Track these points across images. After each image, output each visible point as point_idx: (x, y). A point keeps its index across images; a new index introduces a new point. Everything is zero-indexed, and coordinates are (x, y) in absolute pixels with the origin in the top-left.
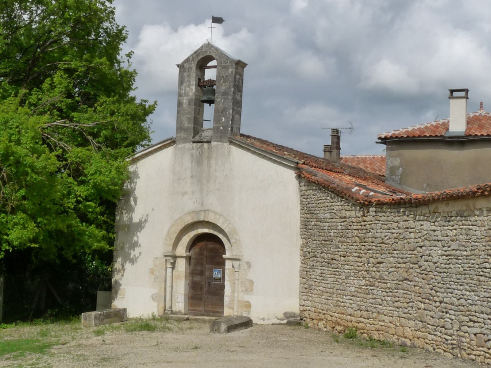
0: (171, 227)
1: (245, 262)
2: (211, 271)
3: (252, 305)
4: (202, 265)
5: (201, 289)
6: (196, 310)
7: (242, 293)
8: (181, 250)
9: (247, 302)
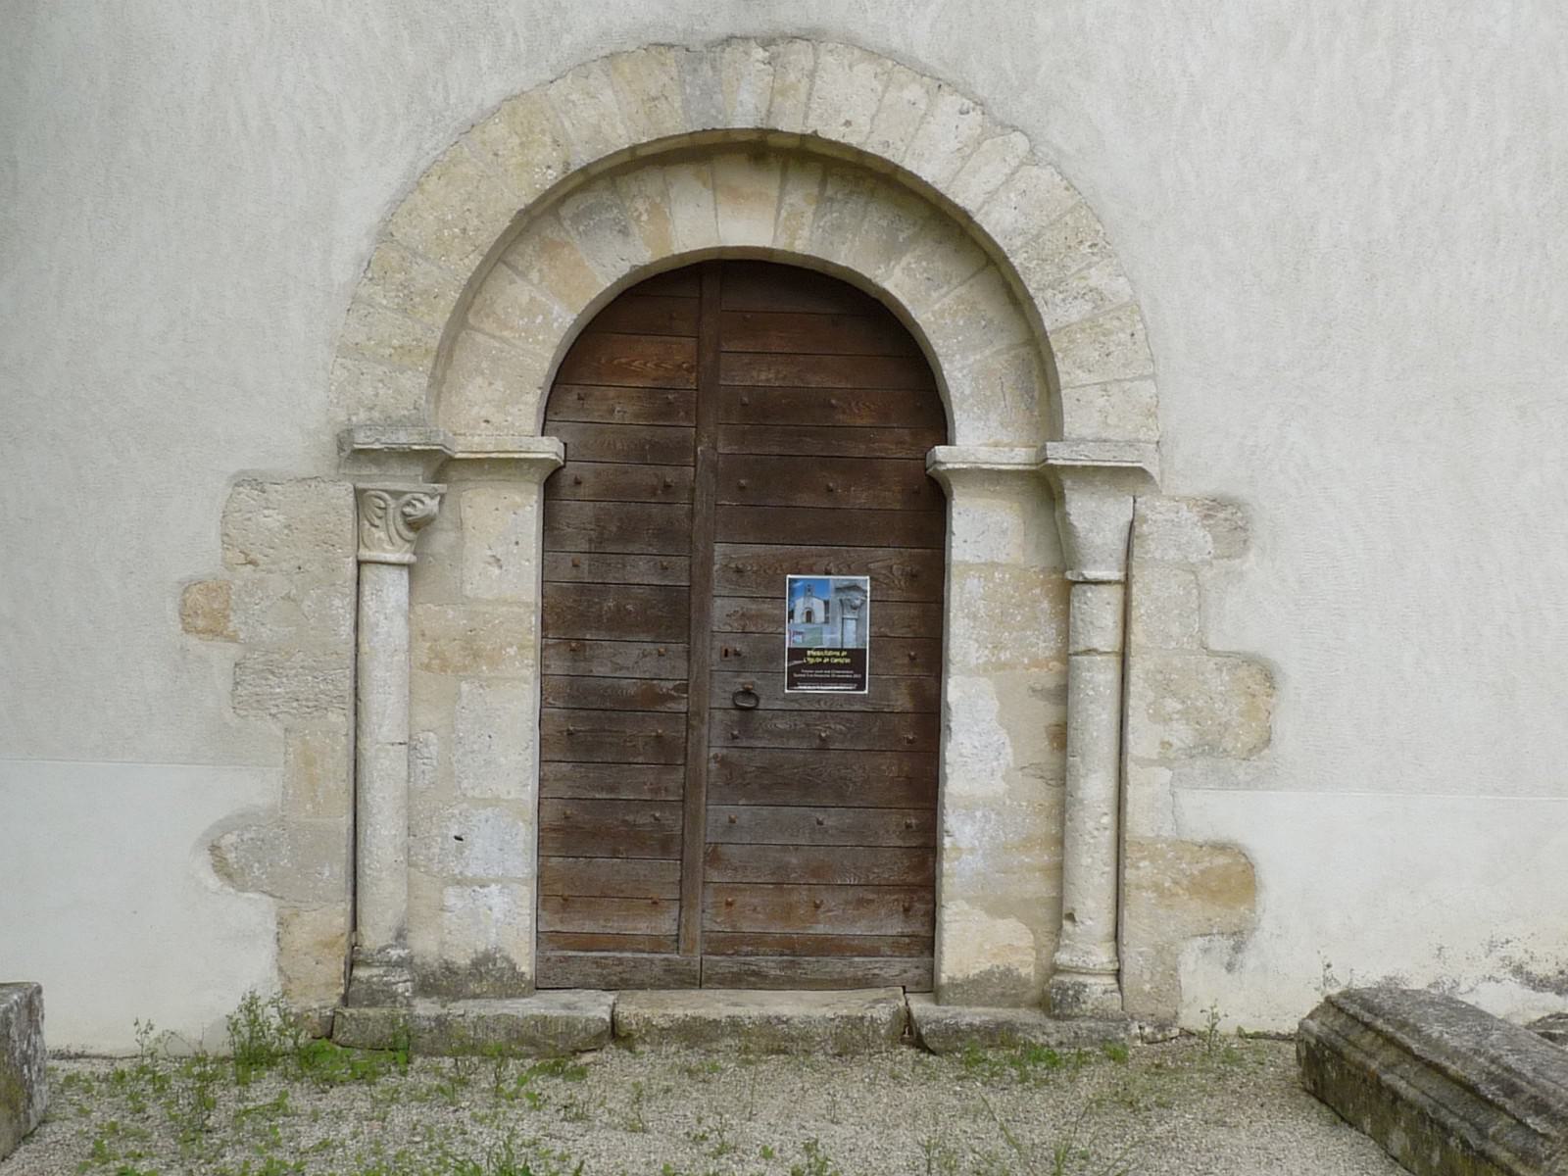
0: (417, 184)
1: (1192, 501)
2: (771, 585)
3: (1267, 874)
4: (670, 537)
5: (669, 752)
6: (620, 942)
7: (1166, 775)
8: (502, 407)
9: (1221, 847)
